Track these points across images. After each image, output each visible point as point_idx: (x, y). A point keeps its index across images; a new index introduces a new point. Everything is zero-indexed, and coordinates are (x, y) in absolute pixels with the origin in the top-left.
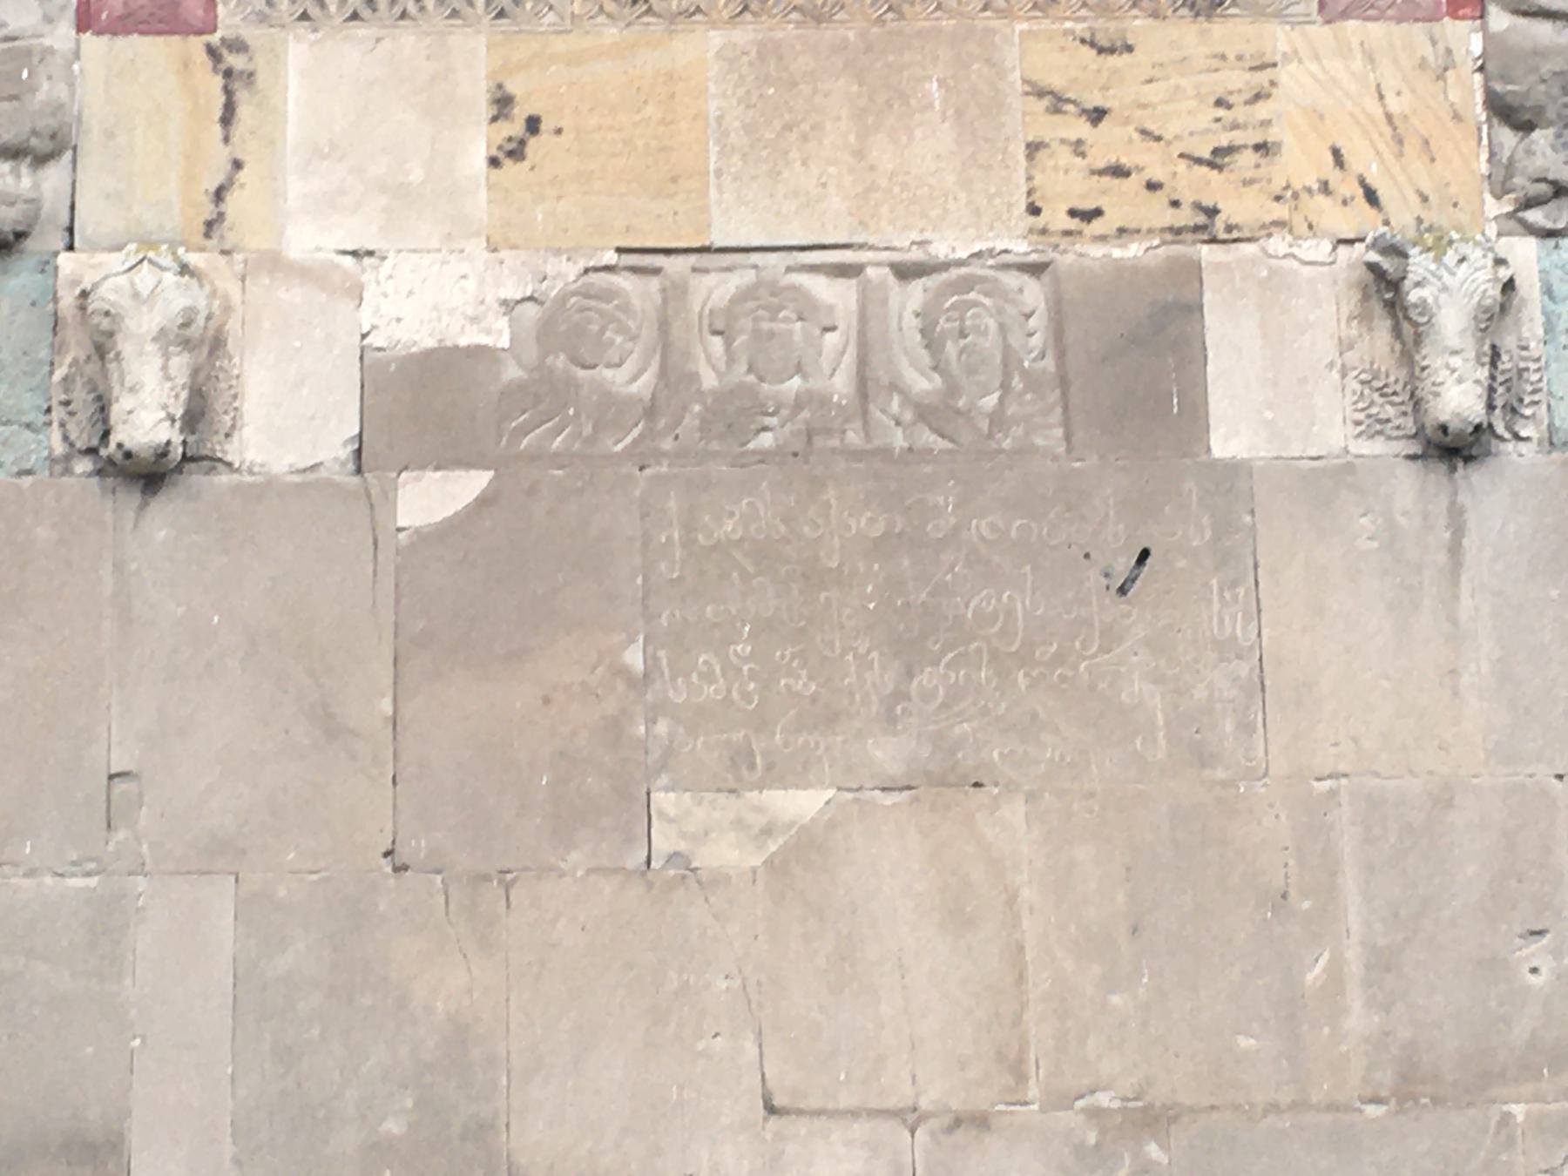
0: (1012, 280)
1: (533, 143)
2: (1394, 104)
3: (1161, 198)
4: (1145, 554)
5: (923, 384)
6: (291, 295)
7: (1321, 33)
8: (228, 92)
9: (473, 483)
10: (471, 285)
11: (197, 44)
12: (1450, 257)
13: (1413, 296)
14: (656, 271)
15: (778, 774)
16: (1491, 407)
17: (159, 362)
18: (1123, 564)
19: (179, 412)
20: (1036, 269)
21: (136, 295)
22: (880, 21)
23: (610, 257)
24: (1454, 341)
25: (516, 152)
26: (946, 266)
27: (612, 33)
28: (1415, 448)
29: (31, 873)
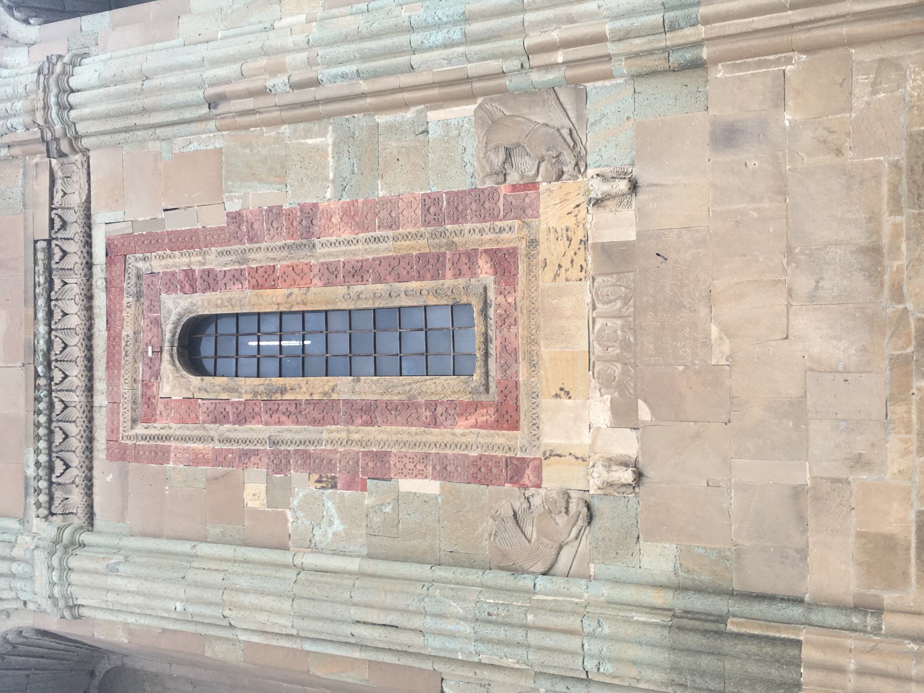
0: (596, 284)
1: (566, 389)
2: (558, 201)
3: (578, 252)
4: (657, 254)
5: (619, 304)
6: (599, 442)
7: (542, 218)
8: (554, 456)
9: (641, 403)
10: (597, 403)
11: (544, 462)
12: (591, 188)
13: (600, 196)
14: (594, 363)
15: (708, 335)
17: (614, 473)
19: (625, 468)
20: (594, 279)
21: (599, 477)
22: (539, 314)
23: (591, 373)
24: (610, 187)
25: (568, 393)
26: (593, 300)
27: (542, 372)
28: (634, 195)
29: (731, 505)
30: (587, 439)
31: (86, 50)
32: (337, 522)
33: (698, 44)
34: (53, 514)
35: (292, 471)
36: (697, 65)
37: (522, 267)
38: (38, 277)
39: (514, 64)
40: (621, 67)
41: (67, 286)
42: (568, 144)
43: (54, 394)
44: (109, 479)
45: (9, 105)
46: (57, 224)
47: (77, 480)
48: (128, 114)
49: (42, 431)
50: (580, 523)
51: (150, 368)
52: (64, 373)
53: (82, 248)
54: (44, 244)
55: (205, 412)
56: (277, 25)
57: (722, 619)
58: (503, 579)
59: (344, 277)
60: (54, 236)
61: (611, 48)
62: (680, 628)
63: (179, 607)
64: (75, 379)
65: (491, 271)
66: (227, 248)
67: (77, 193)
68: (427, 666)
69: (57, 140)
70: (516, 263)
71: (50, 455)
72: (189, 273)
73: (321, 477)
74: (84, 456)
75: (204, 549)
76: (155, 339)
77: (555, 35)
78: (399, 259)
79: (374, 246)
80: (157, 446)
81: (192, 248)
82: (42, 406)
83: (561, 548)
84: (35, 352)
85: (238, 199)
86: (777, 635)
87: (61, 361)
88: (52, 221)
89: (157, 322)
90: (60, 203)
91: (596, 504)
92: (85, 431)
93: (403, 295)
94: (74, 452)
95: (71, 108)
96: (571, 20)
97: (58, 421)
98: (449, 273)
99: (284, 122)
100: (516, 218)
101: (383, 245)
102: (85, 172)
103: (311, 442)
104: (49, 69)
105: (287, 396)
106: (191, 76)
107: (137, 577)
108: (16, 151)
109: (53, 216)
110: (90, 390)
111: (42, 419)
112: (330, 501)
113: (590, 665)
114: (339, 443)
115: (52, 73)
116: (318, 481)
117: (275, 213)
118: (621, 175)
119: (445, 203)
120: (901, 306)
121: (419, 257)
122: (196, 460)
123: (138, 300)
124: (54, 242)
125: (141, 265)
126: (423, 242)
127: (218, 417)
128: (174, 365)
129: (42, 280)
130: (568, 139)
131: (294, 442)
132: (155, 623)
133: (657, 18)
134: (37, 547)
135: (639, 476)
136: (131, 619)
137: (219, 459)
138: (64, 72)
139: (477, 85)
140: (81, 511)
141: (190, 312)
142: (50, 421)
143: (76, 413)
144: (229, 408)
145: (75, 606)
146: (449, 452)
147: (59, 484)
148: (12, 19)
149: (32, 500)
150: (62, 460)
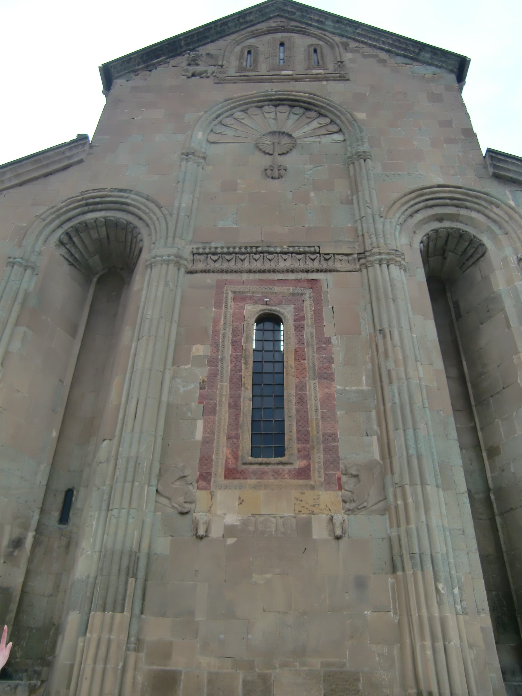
1: (243, 503)
2: (333, 500)
5: (283, 530)
10: (236, 518)
11: (209, 492)
16: (342, 533)
18: (303, 550)
20: (295, 517)
23: (250, 515)
30: (219, 512)
31: (407, 271)
32: (184, 389)
33: (403, 570)
34: (194, 255)
35: (208, 368)
36: (394, 570)
37: (301, 482)
38: (303, 248)
39: (397, 480)
40: (394, 533)
41: (298, 261)
42: (359, 505)
43: (248, 255)
44: (208, 280)
45: (382, 236)
46: (327, 258)
47: (208, 266)
48: (377, 291)
49: (231, 250)
50: (180, 509)
51: (259, 300)
52: (258, 260)
53: (316, 268)
54: (318, 251)
55: (237, 326)
56: (419, 363)
57: (135, 576)
58: (156, 470)
59: (299, 394)
60: (321, 255)
61: (403, 527)
62: (130, 556)
63: (149, 317)
64: (255, 265)
65: (300, 466)
66: (314, 337)
67: (341, 266)
68: (117, 433)
69: (365, 258)
70: (304, 479)
71: (220, 253)
72: (303, 318)
73: (205, 382)
74: (219, 269)
75: (174, 327)
76: (272, 302)
77: (410, 500)
78: (307, 421)
79: (314, 409)
80: (223, 303)
81: (315, 320)
82: (243, 250)
83: (169, 499)
84: (268, 246)
85: (338, 343)
86: (127, 601)
87: (264, 258)
88: (328, 254)
89: (280, 303)
90: (337, 258)
91: (188, 516)
92: (231, 269)
93: (290, 423)
94: (222, 264)
95: (380, 265)
96: (417, 508)
97: (236, 257)
98: (300, 446)
99: (373, 365)
100: (325, 479)
101: (314, 414)
102: (351, 270)
103: (222, 377)
104: (398, 255)
105: (243, 366)
106: (395, 322)
107: (163, 295)
108: (361, 238)
109: (330, 255)
110: (250, 271)
111: (237, 250)
112: (194, 387)
113: (115, 512)
114: (221, 391)
115: (396, 256)
116: (203, 381)
117: (330, 360)
118: (344, 532)
119: (333, 444)
120: (277, 666)
121: (308, 431)
122: (216, 322)
123: (291, 294)
124: (318, 255)
125: (307, 295)
126: (315, 433)
127: (235, 332)
128: (260, 311)
129: (301, 249)
130: (362, 506)
131: (222, 369)
132: (142, 304)
133: (417, 550)
134: (179, 249)
135: (201, 538)
136: (144, 292)
137: (216, 332)
138: (397, 262)
139: (388, 461)
140: (194, 268)
141: (284, 319)
142: (236, 253)
143: (239, 266)
144: (239, 338)
145: (152, 266)
146: (215, 444)
147: (207, 257)
148: (422, 236)
149: (200, 245)
150: (218, 259)
